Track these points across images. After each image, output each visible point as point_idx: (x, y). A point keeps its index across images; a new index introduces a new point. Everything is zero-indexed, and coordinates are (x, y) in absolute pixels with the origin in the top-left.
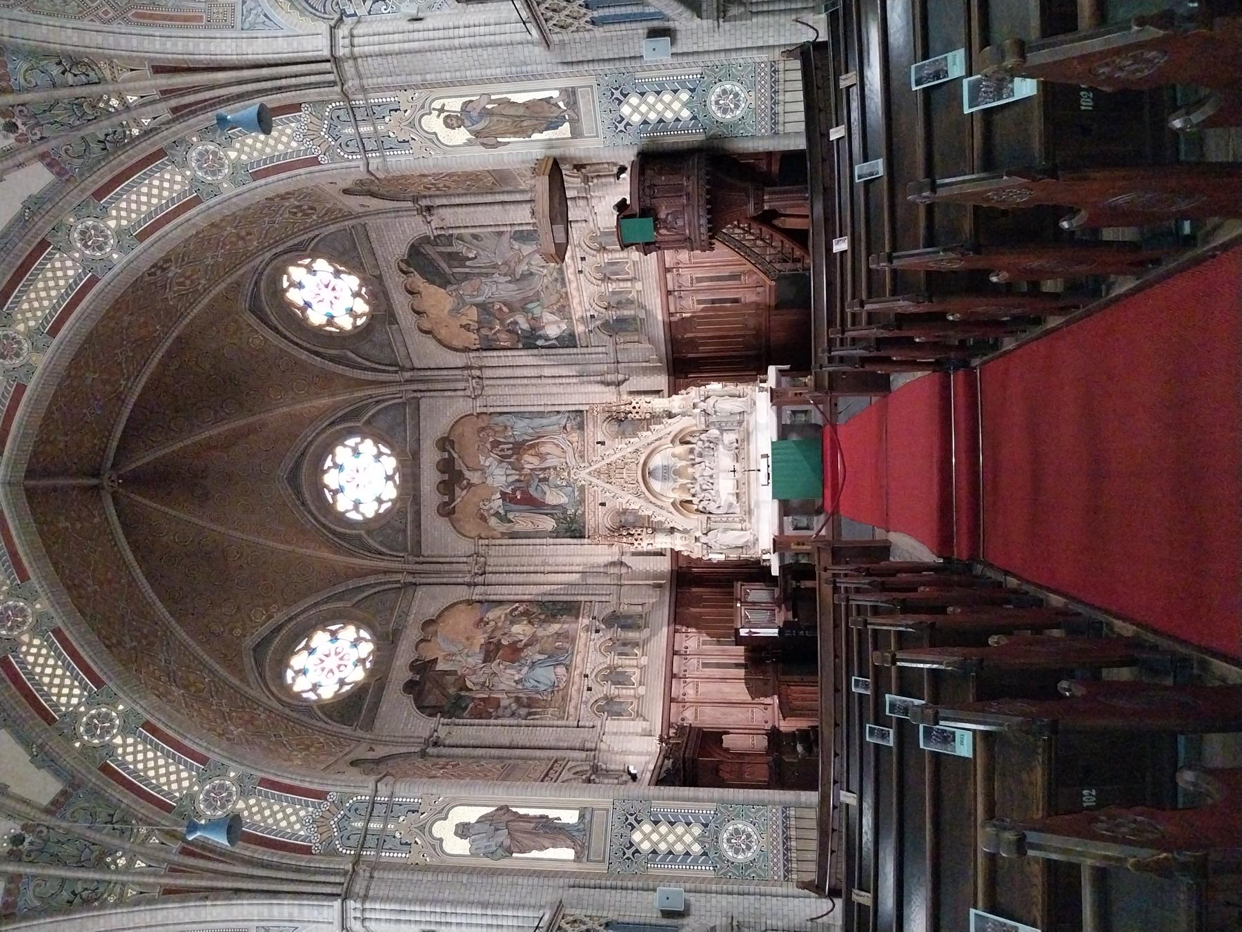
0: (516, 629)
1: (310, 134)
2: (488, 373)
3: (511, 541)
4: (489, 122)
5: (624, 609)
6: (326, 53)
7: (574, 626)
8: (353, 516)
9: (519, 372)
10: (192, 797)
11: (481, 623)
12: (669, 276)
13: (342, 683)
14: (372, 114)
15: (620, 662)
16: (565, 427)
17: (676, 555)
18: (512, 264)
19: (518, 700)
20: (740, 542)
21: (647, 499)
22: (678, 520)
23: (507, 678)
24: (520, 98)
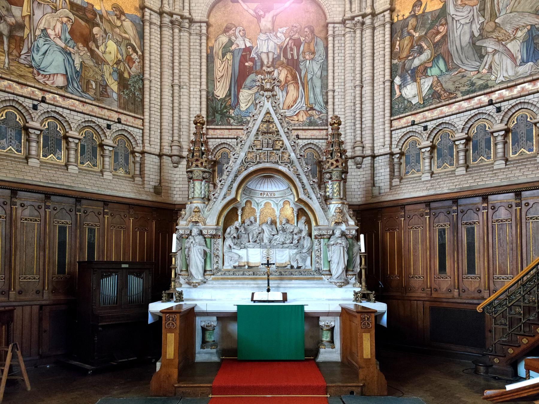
0: (112, 46)
2: (368, 33)
3: (204, 54)
7: (116, 103)
12: (478, 200)
15: (73, 145)
16: (312, 109)
18: (494, 35)
19: (21, 26)
20: (193, 270)
21: (239, 172)
22: (218, 205)
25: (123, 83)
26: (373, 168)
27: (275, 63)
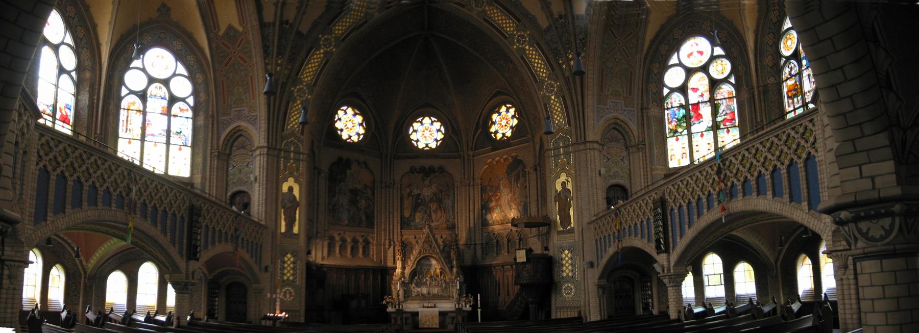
0: (363, 201)
1: (560, 129)
2: (471, 189)
4: (563, 198)
5: (371, 247)
6: (587, 139)
8: (411, 130)
9: (471, 202)
10: (301, 83)
11: (366, 186)
13: (342, 130)
14: (567, 154)
17: (395, 269)
23: (344, 200)
24: (571, 212)
25: (367, 217)
26: (475, 249)
27: (431, 201)
